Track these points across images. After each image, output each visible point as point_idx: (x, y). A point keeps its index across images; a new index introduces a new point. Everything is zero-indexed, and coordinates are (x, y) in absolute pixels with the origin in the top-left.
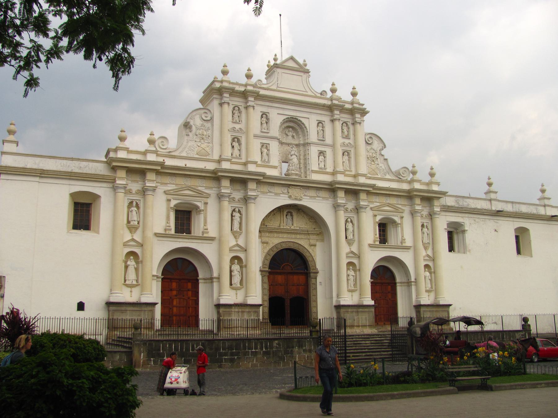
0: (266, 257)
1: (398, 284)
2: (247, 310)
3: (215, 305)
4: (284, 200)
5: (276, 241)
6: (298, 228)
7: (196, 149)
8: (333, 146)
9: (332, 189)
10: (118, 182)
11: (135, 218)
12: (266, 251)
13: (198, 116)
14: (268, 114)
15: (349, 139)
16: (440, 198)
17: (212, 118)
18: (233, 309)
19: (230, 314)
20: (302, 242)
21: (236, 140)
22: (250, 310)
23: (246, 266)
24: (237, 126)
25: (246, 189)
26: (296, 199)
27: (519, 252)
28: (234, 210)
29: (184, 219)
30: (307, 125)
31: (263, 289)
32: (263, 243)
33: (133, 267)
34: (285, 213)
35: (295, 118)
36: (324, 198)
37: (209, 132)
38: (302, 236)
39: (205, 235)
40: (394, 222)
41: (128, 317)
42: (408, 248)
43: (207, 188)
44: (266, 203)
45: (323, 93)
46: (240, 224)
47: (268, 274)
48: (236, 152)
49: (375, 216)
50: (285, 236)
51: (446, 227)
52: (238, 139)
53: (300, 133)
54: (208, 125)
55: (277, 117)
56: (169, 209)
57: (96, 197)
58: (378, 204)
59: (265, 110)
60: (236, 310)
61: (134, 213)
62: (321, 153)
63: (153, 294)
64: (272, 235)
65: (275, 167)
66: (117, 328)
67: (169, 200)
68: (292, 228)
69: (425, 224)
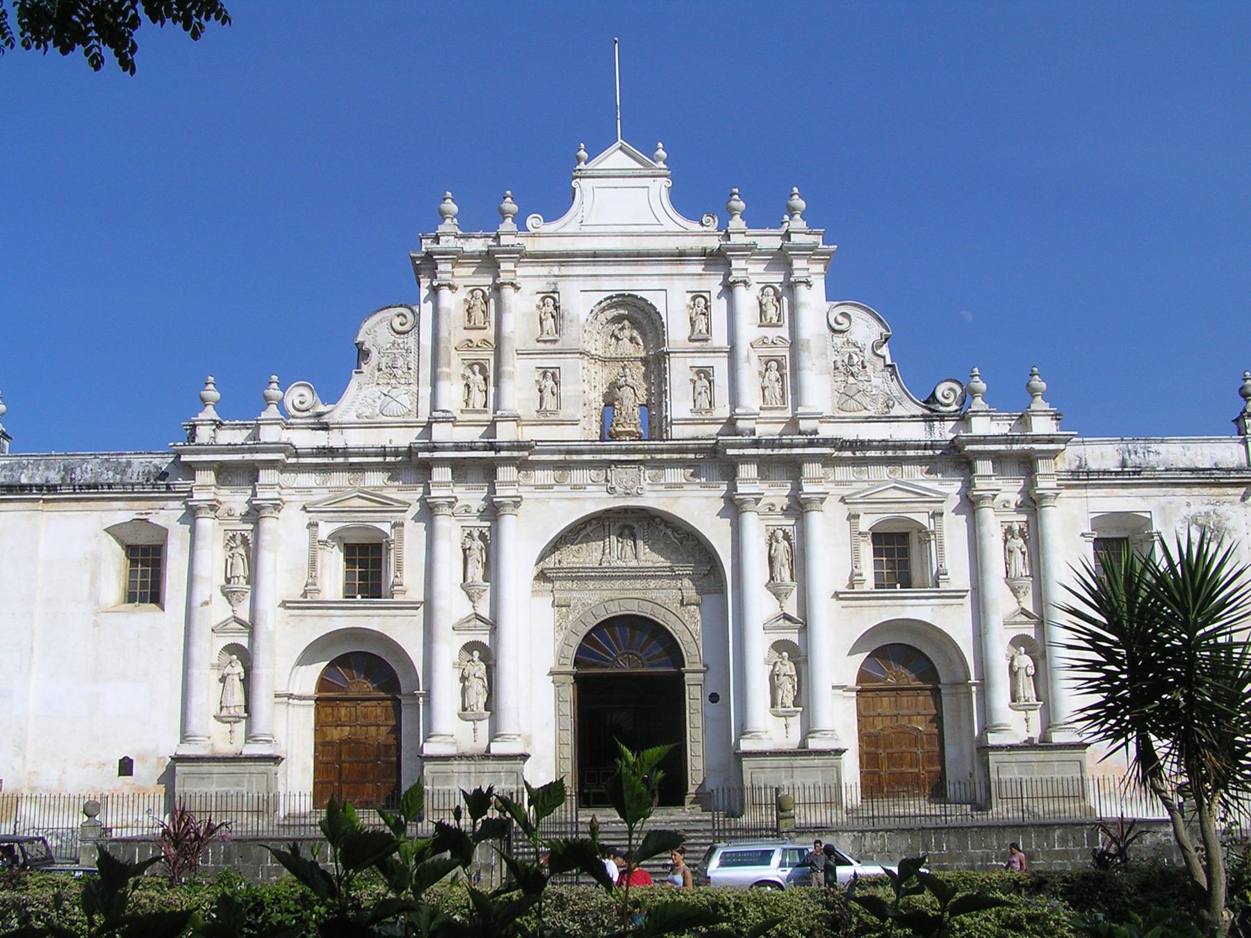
4: (594, 500)
6: (650, 564)
8: (732, 353)
10: (196, 497)
13: (385, 324)
14: (556, 296)
17: (417, 325)
18: (456, 766)
19: (447, 777)
28: (470, 535)
29: (367, 563)
30: (661, 309)
31: (559, 714)
33: (236, 678)
39: (397, 598)
40: (921, 529)
41: (213, 789)
42: (958, 595)
44: (540, 511)
47: (571, 679)
48: (478, 399)
49: (853, 517)
50: (617, 584)
51: (1088, 530)
54: (411, 340)
55: (582, 297)
56: (316, 545)
58: (865, 486)
60: (464, 768)
61: (238, 560)
63: (293, 735)
64: (582, 584)
65: (574, 423)
67: (313, 525)
68: (634, 563)
69: (1016, 527)
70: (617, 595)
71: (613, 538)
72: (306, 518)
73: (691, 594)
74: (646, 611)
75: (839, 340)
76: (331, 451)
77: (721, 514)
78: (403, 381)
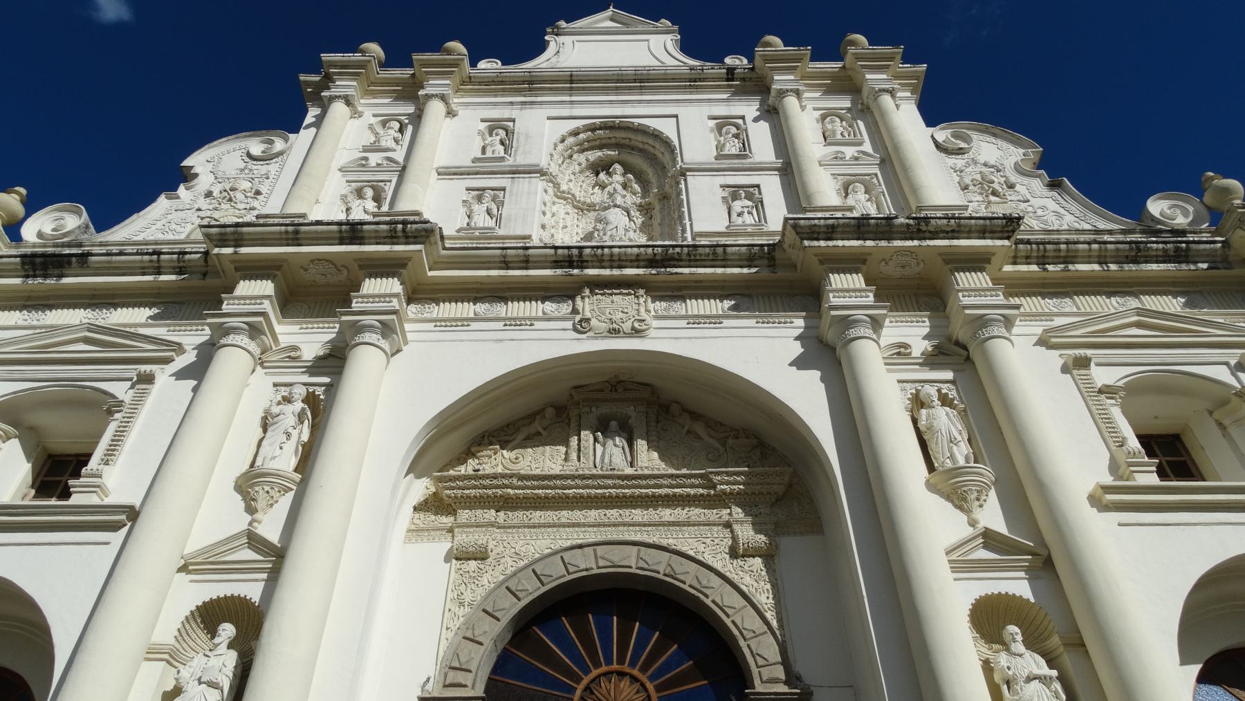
0: (469, 624)
5: (537, 549)
12: (475, 594)
15: (860, 144)
20: (686, 542)
26: (614, 332)
32: (460, 556)
38: (696, 513)
50: (593, 515)
70: (592, 536)
71: (587, 435)
73: (747, 534)
75: (959, 161)
77: (800, 363)
78: (242, 206)
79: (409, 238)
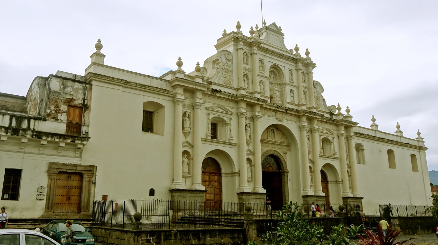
1: (329, 183)
2: (259, 197)
3: (238, 194)
4: (273, 121)
7: (223, 79)
9: (298, 115)
11: (188, 126)
16: (354, 127)
20: (279, 151)
21: (246, 76)
22: (260, 197)
23: (254, 166)
24: (247, 67)
25: (253, 111)
27: (391, 166)
34: (270, 130)
35: (277, 66)
36: (294, 122)
37: (230, 68)
38: (279, 147)
39: (231, 142)
43: (230, 107)
44: (265, 121)
45: (291, 51)
46: (250, 136)
50: (270, 145)
52: (247, 76)
53: (278, 76)
54: (230, 63)
57: (160, 107)
59: (261, 57)
60: (253, 197)
61: (187, 121)
62: (291, 91)
66: (179, 210)
72: (206, 111)
74: (276, 154)
76: (216, 91)
79: (264, 102)
